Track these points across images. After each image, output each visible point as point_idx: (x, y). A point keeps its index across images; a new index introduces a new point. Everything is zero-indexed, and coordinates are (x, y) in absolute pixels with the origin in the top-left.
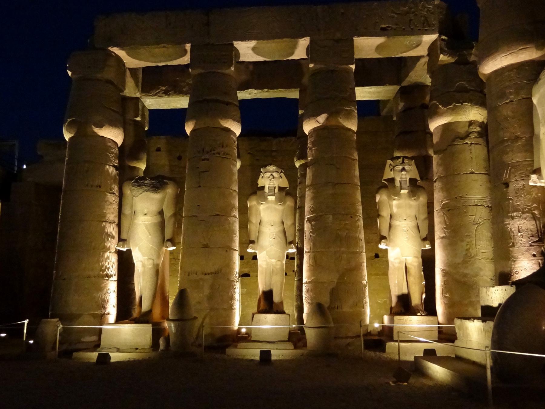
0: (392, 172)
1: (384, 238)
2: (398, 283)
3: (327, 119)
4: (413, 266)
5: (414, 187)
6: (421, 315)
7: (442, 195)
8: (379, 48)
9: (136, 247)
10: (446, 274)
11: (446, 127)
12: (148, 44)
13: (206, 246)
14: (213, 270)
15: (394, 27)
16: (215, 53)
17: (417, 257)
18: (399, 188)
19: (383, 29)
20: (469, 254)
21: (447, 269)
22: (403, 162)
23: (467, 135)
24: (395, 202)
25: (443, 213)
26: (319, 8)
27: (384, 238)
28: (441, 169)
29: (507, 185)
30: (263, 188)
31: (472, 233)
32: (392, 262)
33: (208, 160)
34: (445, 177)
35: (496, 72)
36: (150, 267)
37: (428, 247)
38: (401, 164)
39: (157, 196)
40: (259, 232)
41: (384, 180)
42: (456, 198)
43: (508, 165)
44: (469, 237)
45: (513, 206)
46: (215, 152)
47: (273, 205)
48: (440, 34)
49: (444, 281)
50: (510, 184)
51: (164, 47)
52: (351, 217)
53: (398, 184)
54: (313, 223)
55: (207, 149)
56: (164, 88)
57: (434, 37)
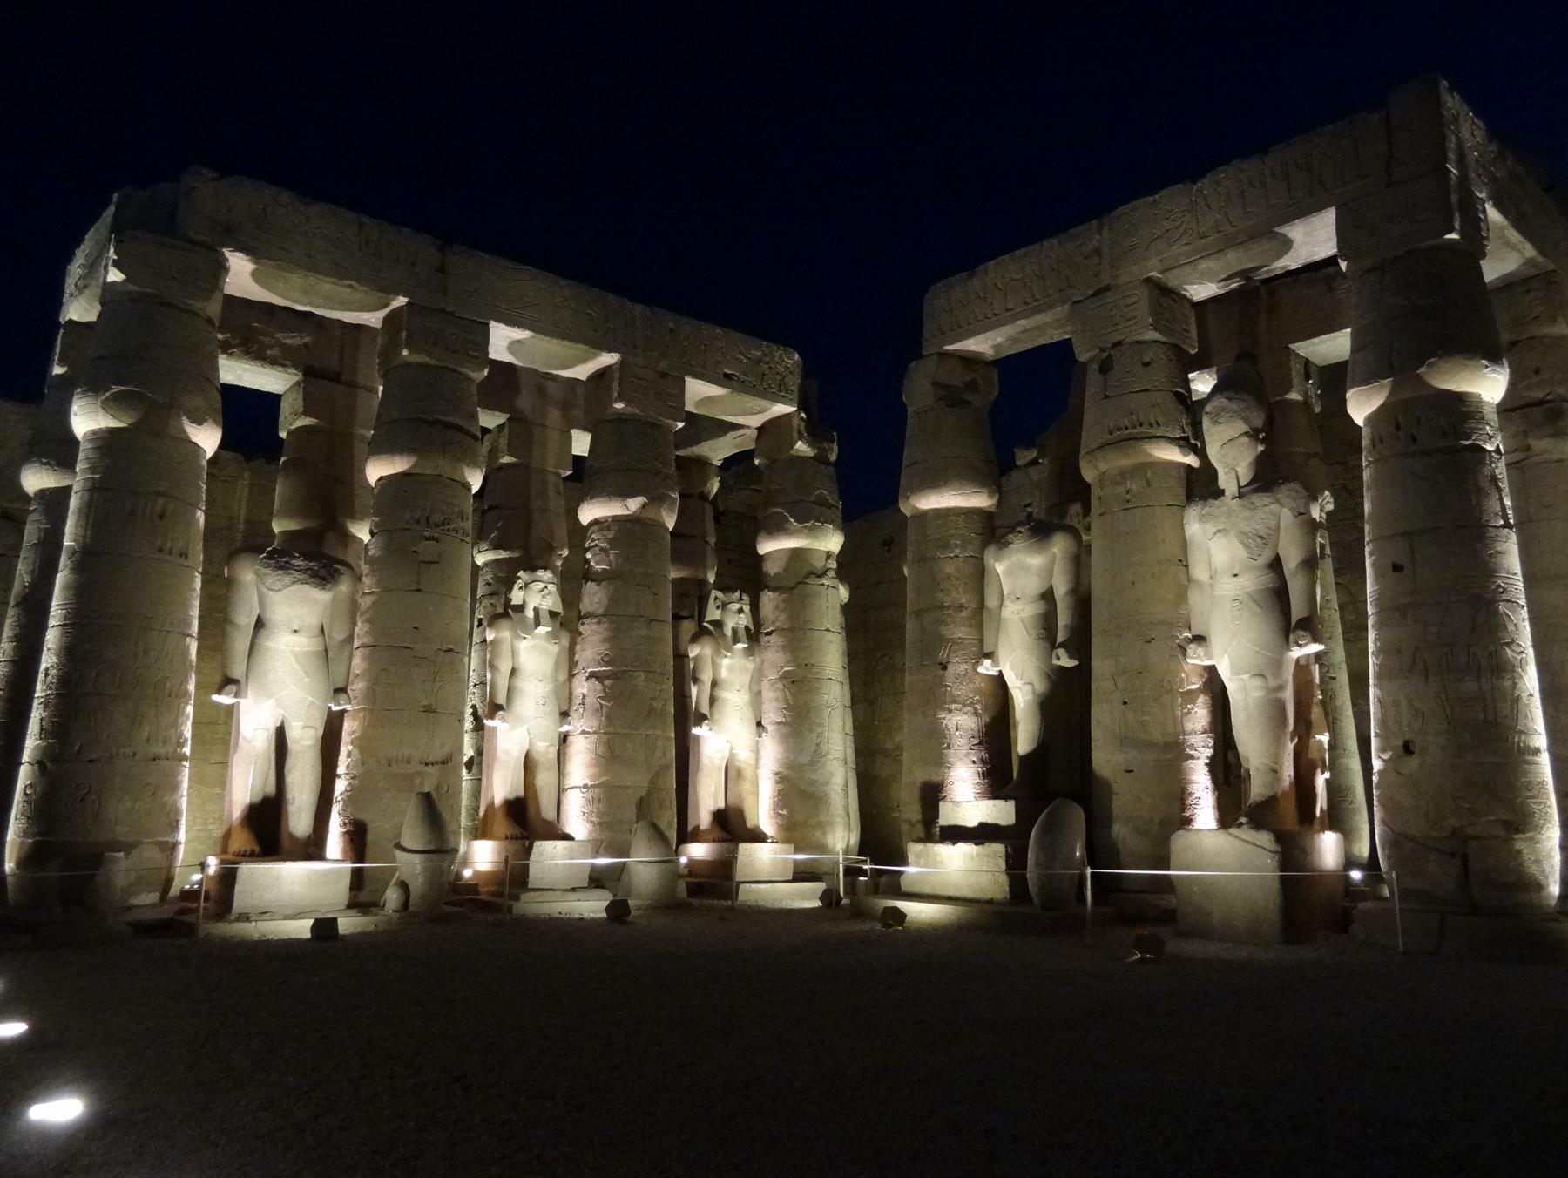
3: (644, 506)
8: (709, 400)
9: (270, 697)
11: (796, 553)
12: (318, 272)
13: (429, 710)
14: (439, 759)
15: (743, 378)
16: (450, 329)
19: (726, 376)
21: (786, 772)
23: (823, 574)
24: (726, 662)
26: (638, 309)
29: (945, 668)
30: (520, 608)
33: (437, 540)
35: (937, 511)
36: (308, 743)
39: (321, 597)
40: (510, 691)
43: (948, 640)
45: (952, 695)
46: (451, 527)
47: (543, 643)
48: (799, 409)
50: (950, 667)
51: (351, 286)
53: (729, 632)
54: (607, 682)
55: (437, 518)
56: (220, 337)
57: (790, 409)
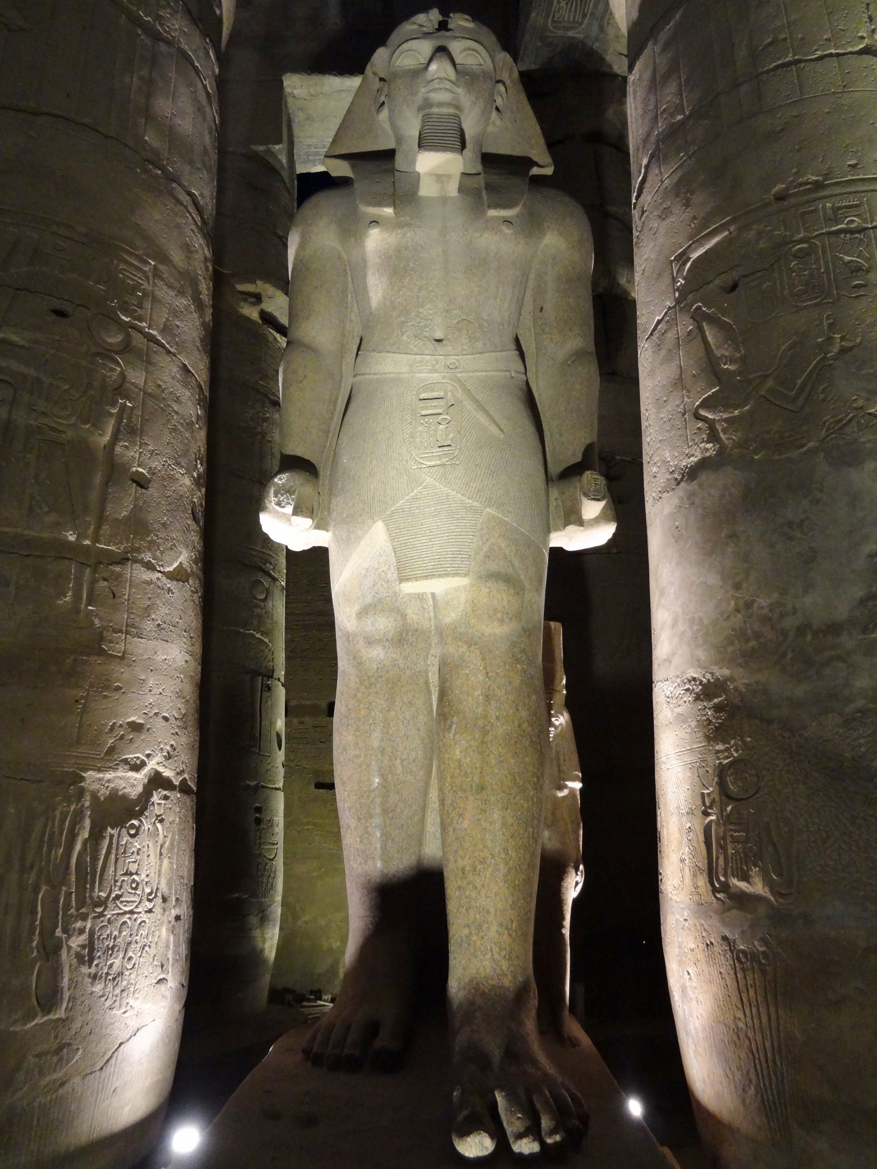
17: (508, 580)
21: (742, 679)
32: (347, 636)
37: (590, 532)
42: (780, 197)
49: (721, 772)
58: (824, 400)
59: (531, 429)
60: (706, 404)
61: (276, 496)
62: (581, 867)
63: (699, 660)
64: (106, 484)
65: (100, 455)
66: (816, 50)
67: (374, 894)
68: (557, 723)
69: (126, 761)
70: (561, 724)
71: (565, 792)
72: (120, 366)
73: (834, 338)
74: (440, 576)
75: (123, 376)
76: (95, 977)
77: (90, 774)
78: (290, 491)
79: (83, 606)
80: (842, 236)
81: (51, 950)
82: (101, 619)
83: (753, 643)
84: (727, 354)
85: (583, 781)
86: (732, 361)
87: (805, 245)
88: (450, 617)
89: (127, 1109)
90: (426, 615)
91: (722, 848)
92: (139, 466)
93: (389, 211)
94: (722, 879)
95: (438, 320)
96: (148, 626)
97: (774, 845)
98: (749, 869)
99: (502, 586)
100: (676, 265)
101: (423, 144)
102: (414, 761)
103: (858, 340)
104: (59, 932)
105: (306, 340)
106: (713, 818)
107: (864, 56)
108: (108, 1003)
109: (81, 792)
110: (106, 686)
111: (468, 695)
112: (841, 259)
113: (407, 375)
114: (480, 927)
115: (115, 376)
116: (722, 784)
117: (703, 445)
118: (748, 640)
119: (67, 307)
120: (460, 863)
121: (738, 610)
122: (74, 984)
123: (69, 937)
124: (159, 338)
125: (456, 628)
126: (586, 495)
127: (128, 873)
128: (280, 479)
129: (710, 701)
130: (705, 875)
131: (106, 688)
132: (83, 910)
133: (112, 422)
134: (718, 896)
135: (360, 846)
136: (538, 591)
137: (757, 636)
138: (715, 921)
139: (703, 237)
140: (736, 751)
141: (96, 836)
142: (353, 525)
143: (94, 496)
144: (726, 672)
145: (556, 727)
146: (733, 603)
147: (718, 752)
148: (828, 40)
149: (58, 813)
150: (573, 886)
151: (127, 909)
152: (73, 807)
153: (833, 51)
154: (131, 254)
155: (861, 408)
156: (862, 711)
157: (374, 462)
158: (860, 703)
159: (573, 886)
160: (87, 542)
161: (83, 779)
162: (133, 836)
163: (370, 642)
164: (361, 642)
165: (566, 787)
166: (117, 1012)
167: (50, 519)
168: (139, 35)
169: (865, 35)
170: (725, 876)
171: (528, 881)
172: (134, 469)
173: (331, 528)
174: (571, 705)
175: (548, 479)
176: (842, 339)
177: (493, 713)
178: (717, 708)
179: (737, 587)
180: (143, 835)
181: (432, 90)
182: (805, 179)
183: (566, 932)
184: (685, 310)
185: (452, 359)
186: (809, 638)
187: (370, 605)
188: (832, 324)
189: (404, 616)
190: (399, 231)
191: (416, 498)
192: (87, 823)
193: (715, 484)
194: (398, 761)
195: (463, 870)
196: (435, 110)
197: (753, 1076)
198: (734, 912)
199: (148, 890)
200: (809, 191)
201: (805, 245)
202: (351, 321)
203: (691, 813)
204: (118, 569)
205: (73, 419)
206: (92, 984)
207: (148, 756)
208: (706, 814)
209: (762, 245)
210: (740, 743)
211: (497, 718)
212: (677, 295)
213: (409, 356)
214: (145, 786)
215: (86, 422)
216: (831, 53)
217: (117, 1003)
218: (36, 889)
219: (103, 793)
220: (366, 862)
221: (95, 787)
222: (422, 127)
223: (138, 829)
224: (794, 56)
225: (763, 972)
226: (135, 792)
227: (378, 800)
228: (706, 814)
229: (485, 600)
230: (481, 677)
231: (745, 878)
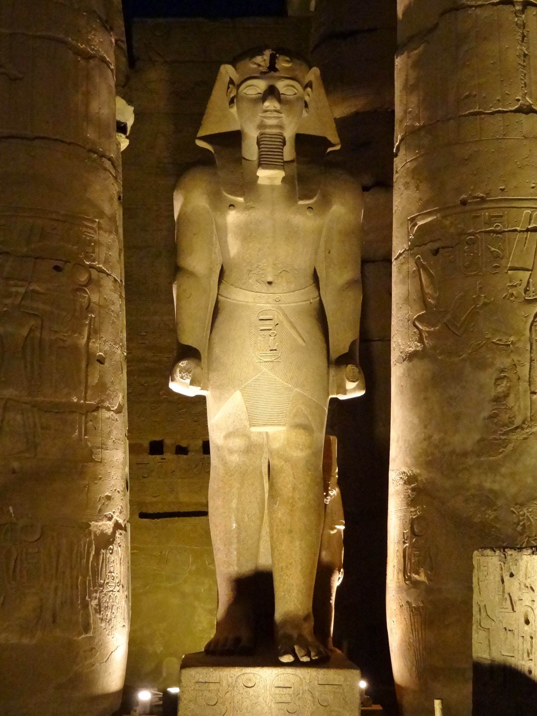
0: (234, 110)
1: (190, 353)
2: (239, 527)
4: (287, 460)
5: (313, 165)
6: (297, 664)
7: (417, 195)
10: (419, 493)
17: (306, 428)
18: (256, 163)
20: (504, 417)
21: (424, 475)
22: (272, 68)
24: (232, 217)
25: (418, 263)
27: (190, 353)
28: (414, 99)
31: (519, 333)
32: (218, 448)
34: (429, 128)
37: (353, 391)
38: (262, 75)
41: (204, 139)
42: (464, 203)
44: (507, 348)
49: (412, 522)
52: (57, 268)
53: (251, 150)
58: (472, 332)
59: (319, 335)
60: (419, 319)
61: (180, 373)
62: (342, 570)
63: (407, 463)
64: (87, 366)
65: (83, 351)
66: (491, 107)
67: (233, 584)
68: (332, 494)
69: (106, 516)
70: (334, 495)
71: (335, 531)
72: (87, 294)
73: (481, 297)
74: (271, 425)
75: (89, 299)
76: (102, 619)
77: (93, 523)
78: (188, 371)
79: (83, 437)
80: (492, 234)
81: (86, 606)
82: (91, 442)
83: (430, 458)
84: (430, 293)
85: (345, 525)
86: (433, 298)
87: (473, 237)
88: (276, 445)
89: (114, 683)
90: (261, 436)
91: (410, 560)
92: (100, 352)
93: (241, 199)
94: (409, 574)
95: (269, 269)
96: (110, 443)
97: (431, 559)
98: (419, 569)
99: (302, 431)
100: (410, 224)
101: (261, 165)
102: (254, 514)
103: (492, 299)
104: (87, 598)
105: (190, 268)
106: (407, 545)
107: (517, 114)
108: (107, 632)
109: (90, 532)
110: (96, 478)
111: (285, 487)
112: (489, 249)
113: (252, 304)
114: (289, 592)
115: (86, 301)
116: (412, 528)
117: (416, 343)
118: (428, 456)
119: (60, 264)
120: (280, 565)
121: (425, 440)
122: (95, 622)
123: (91, 600)
124: (103, 268)
125: (279, 451)
126: (348, 379)
127: (110, 572)
128: (183, 364)
129: (410, 485)
130: (402, 572)
131: (96, 479)
132: (96, 588)
133: (87, 329)
134: (407, 582)
135: (225, 559)
136: (321, 432)
137: (432, 454)
138: (404, 594)
139: (424, 214)
140: (419, 512)
141: (97, 554)
142: (223, 388)
143: (83, 374)
144: (418, 471)
145: (331, 497)
146: (423, 435)
147: (411, 512)
148: (499, 100)
149: (82, 543)
150: (337, 580)
151: (111, 589)
152: (88, 539)
153: (500, 109)
154: (86, 220)
155: (489, 339)
156: (473, 496)
157: (235, 356)
158: (473, 491)
159: (337, 580)
160: (82, 401)
161: (90, 526)
162: (111, 554)
163: (231, 452)
164: (226, 452)
165: (335, 528)
166: (110, 637)
167: (66, 391)
168: (79, 61)
169: (520, 98)
170: (410, 573)
171: (311, 573)
172: (98, 354)
173: (210, 389)
174: (340, 483)
175: (329, 362)
176: (485, 297)
177: (297, 496)
178: (413, 490)
179: (425, 427)
180: (114, 554)
181: (265, 117)
182: (477, 194)
183: (333, 602)
184: (413, 255)
185: (277, 296)
186: (454, 458)
187: (231, 432)
188: (481, 288)
189: (249, 438)
190: (247, 212)
191: (257, 379)
192: (94, 546)
193: (420, 365)
194: (246, 516)
195: (282, 568)
196: (268, 131)
197: (415, 663)
198: (412, 590)
199: (117, 581)
200: (477, 203)
201: (473, 237)
202: (215, 253)
203: (399, 542)
204: (95, 414)
205: (70, 333)
206: (101, 623)
207: (114, 512)
208: (404, 543)
209: (452, 230)
210: (421, 508)
211: (299, 499)
212: (410, 244)
213: (253, 293)
214: (113, 528)
215: (75, 333)
216: (500, 110)
217: (110, 633)
218: (77, 578)
219: (98, 532)
220: (229, 567)
221: (95, 529)
222: (260, 152)
223: (112, 550)
224: (479, 109)
225: (421, 615)
226: (109, 531)
227: (235, 536)
228: (404, 543)
229: (294, 439)
230: (291, 478)
231: (418, 573)
